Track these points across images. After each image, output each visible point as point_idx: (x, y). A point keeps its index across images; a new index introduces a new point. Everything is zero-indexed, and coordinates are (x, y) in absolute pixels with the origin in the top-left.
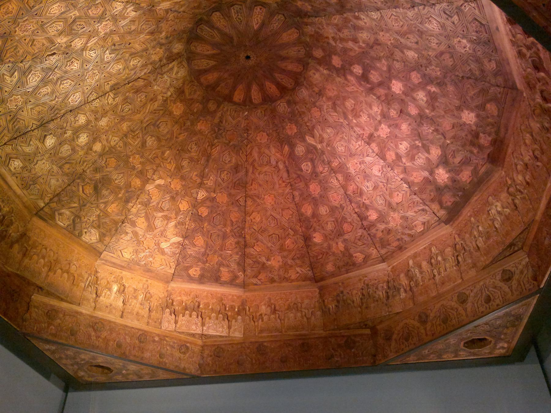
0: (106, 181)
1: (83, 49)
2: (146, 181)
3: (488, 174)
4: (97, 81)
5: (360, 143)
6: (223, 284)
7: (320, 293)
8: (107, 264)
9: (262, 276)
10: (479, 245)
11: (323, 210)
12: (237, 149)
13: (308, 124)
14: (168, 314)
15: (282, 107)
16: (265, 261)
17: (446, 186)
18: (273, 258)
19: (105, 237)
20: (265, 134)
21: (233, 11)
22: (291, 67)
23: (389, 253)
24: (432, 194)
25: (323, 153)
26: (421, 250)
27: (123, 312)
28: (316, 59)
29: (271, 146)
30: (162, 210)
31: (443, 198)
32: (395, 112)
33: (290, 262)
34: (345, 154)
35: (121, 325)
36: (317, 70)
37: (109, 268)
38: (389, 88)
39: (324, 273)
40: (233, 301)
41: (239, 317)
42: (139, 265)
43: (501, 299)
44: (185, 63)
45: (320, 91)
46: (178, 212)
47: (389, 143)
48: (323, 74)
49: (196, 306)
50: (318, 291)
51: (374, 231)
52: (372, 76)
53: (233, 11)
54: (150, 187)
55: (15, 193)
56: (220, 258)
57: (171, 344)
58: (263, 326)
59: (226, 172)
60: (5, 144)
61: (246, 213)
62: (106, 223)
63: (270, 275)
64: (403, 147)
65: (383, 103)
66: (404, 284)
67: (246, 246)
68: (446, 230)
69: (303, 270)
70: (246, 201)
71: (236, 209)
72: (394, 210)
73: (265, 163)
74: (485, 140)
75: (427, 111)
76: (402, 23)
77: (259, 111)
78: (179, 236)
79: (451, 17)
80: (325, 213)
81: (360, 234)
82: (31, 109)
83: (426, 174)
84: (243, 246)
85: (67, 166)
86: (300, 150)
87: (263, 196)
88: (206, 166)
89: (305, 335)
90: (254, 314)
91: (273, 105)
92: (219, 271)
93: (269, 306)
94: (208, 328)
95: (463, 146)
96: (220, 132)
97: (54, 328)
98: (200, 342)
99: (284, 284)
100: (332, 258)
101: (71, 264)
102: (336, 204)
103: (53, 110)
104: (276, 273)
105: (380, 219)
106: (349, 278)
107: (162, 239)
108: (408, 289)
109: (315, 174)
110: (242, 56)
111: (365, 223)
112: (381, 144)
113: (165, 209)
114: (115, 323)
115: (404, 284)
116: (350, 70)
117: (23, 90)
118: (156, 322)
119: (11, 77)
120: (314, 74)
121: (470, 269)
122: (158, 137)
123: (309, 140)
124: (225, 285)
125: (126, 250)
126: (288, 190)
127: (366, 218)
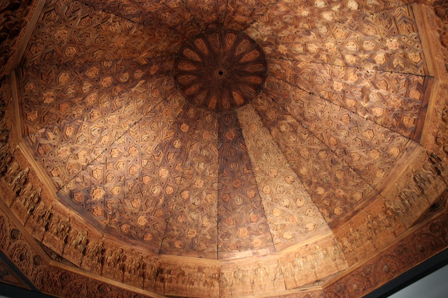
11: (86, 87)
12: (173, 28)
15: (169, 65)
18: (66, 32)
22: (193, 89)
23: (31, 144)
32: (145, 164)
36: (180, 105)
44: (255, 39)
53: (253, 91)
65: (151, 155)
70: (133, 22)
75: (146, 191)
86: (139, 74)
91: (174, 59)
102: (88, 99)
105: (65, 137)
106: (14, 106)
109: (116, 83)
110: (224, 71)
116: (177, 137)
120: (179, 101)
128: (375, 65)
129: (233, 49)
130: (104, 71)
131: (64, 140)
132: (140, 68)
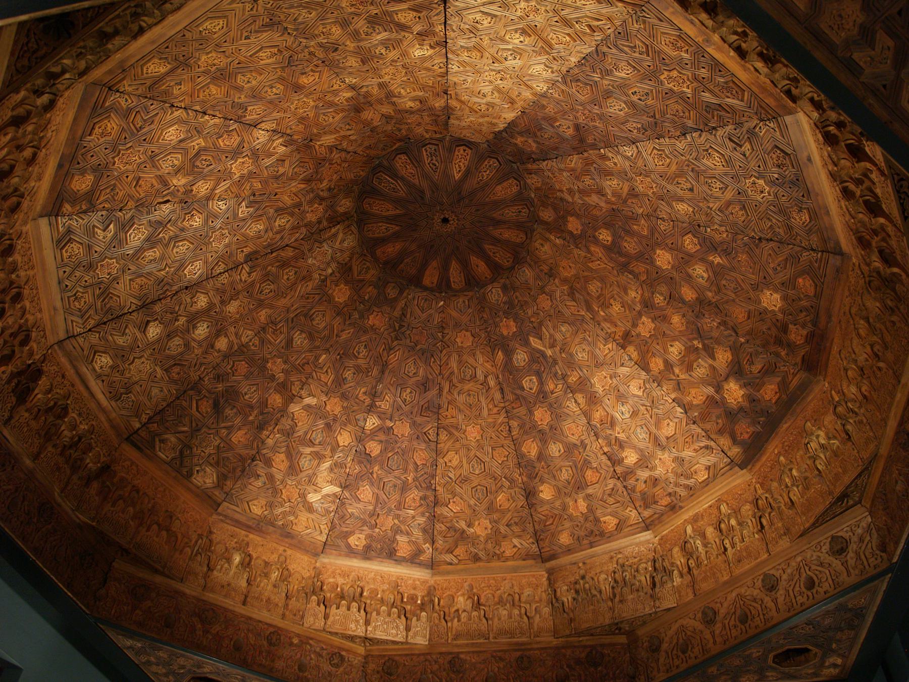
0: (232, 394)
1: (209, 198)
2: (291, 398)
3: (804, 388)
4: (227, 246)
5: (610, 346)
6: (400, 561)
7: (549, 579)
8: (228, 521)
9: (460, 551)
10: (794, 498)
11: (555, 449)
12: (426, 355)
13: (533, 319)
14: (314, 604)
15: (495, 294)
16: (465, 527)
17: (741, 409)
18: (477, 523)
19: (225, 480)
20: (468, 334)
21: (425, 153)
22: (507, 234)
24: (720, 421)
25: (555, 362)
26: (705, 510)
27: (246, 597)
28: (546, 223)
29: (478, 352)
30: (311, 443)
31: (737, 427)
33: (503, 529)
34: (588, 364)
35: (243, 616)
36: (547, 240)
37: (230, 527)
38: (652, 262)
39: (555, 548)
40: (414, 589)
41: (424, 614)
42: (273, 525)
43: (831, 582)
45: (551, 269)
46: (335, 448)
47: (654, 344)
48: (555, 245)
49: (357, 594)
50: (546, 575)
51: (631, 482)
52: (625, 244)
53: (425, 153)
54: (295, 408)
55: (98, 403)
56: (396, 521)
57: (318, 650)
58: (460, 628)
59: (409, 390)
60: (90, 330)
61: (438, 452)
62: (228, 458)
63: (472, 549)
64: (675, 350)
65: (644, 286)
66: (679, 563)
67: (436, 503)
68: (741, 479)
69: (523, 543)
70: (438, 434)
71: (423, 446)
72: (663, 448)
73: (468, 377)
74: (797, 335)
75: (710, 294)
76: (668, 160)
77: (461, 300)
78: (336, 485)
79: (741, 146)
80: (557, 454)
81: (611, 486)
82: (130, 280)
83: (710, 391)
84: (433, 503)
85: (176, 369)
86: (521, 357)
87: (464, 427)
88: (379, 380)
89: (522, 644)
90: (446, 610)
91: (482, 291)
92: (394, 540)
93: (469, 597)
94: (375, 628)
95: (764, 346)
96: (403, 329)
97: (141, 613)
98: (361, 650)
99: (496, 564)
100: (567, 524)
101: (174, 518)
102: (573, 439)
103: (162, 284)
104: (482, 547)
106: (592, 556)
107: (310, 488)
108: (686, 570)
109: (542, 395)
110: (438, 219)
111: (619, 469)
112: (643, 347)
113: (317, 442)
114: (233, 612)
115: (679, 563)
116: (594, 237)
117: (121, 251)
118: (295, 615)
119: (104, 231)
121: (780, 537)
122: (310, 334)
123: (535, 342)
124: (403, 563)
125: (255, 502)
126: (501, 418)
127: (620, 461)
128: (151, 217)
129: (396, 236)
130: (527, 426)
131: (645, 465)
132: (511, 359)
